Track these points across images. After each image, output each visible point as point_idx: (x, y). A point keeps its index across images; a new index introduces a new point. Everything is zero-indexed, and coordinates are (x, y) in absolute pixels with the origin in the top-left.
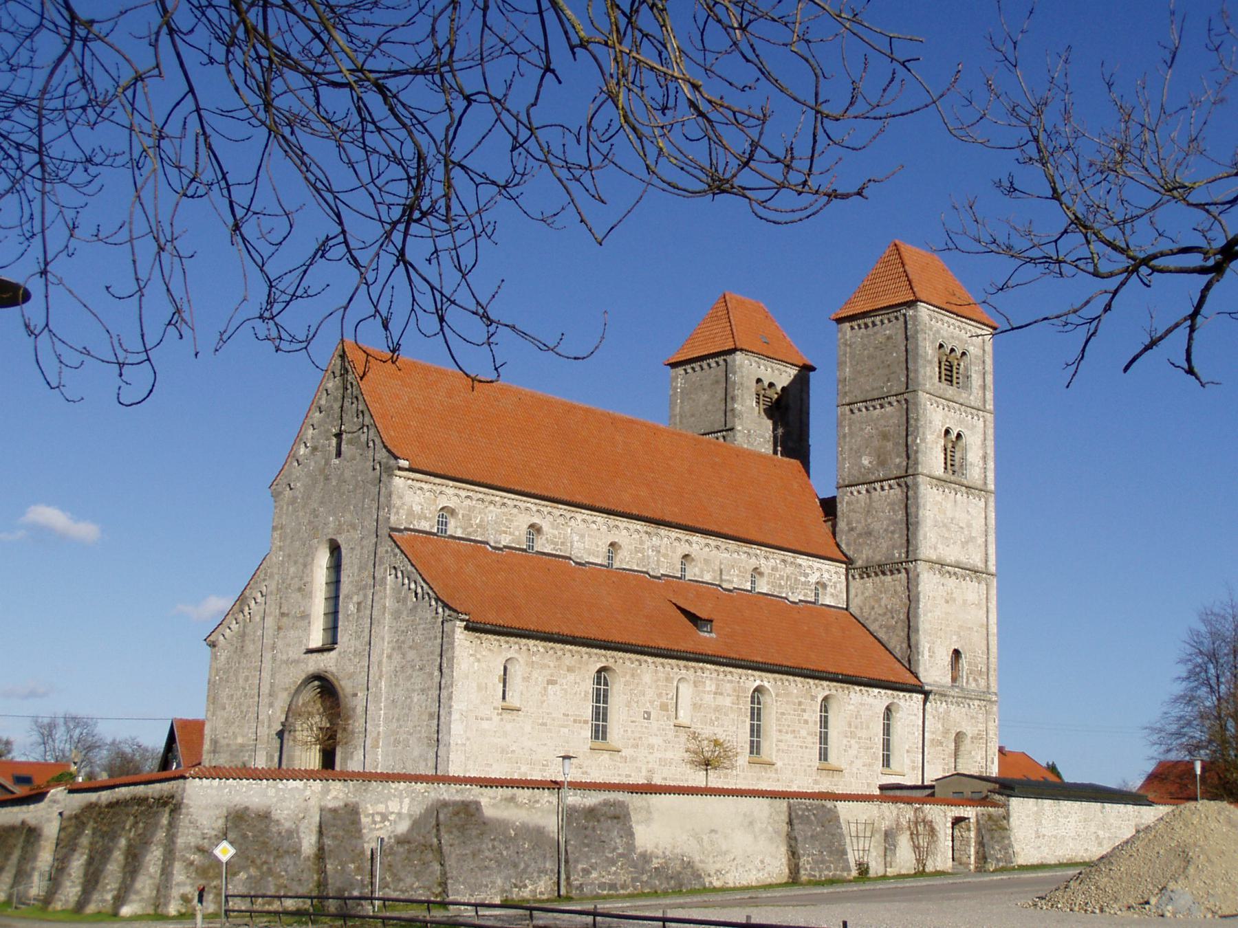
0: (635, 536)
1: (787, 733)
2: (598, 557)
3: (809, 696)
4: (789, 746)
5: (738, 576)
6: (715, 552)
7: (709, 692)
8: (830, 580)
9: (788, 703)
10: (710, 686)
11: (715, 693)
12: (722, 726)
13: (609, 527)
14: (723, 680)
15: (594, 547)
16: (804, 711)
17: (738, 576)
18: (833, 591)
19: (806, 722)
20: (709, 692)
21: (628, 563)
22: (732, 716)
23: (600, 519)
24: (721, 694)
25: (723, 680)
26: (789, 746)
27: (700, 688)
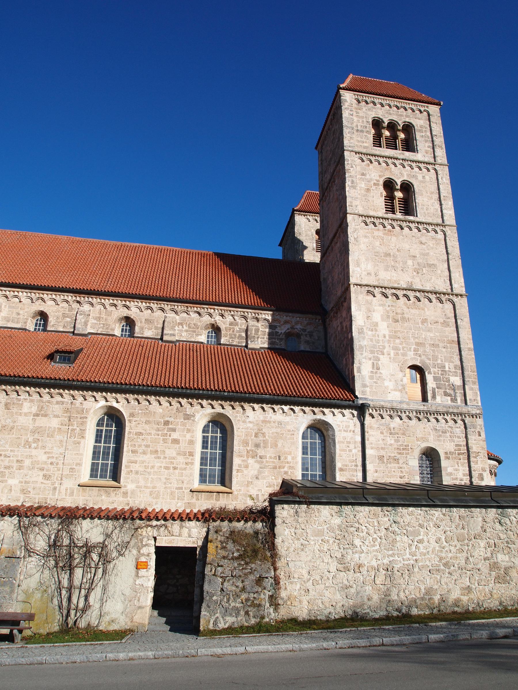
0: (65, 304)
1: (144, 453)
2: (17, 323)
3: (181, 414)
4: (146, 467)
5: (186, 331)
6: (160, 313)
7: (26, 414)
8: (304, 330)
9: (147, 422)
10: (27, 407)
11: (38, 415)
12: (44, 447)
13: (32, 299)
14: (49, 402)
15: (14, 315)
16: (174, 430)
17: (186, 331)
18: (308, 339)
19: (176, 441)
20: (26, 414)
21: (53, 326)
22: (58, 437)
23: (23, 294)
24: (46, 416)
25: (49, 402)
26: (146, 467)
27: (15, 410)
